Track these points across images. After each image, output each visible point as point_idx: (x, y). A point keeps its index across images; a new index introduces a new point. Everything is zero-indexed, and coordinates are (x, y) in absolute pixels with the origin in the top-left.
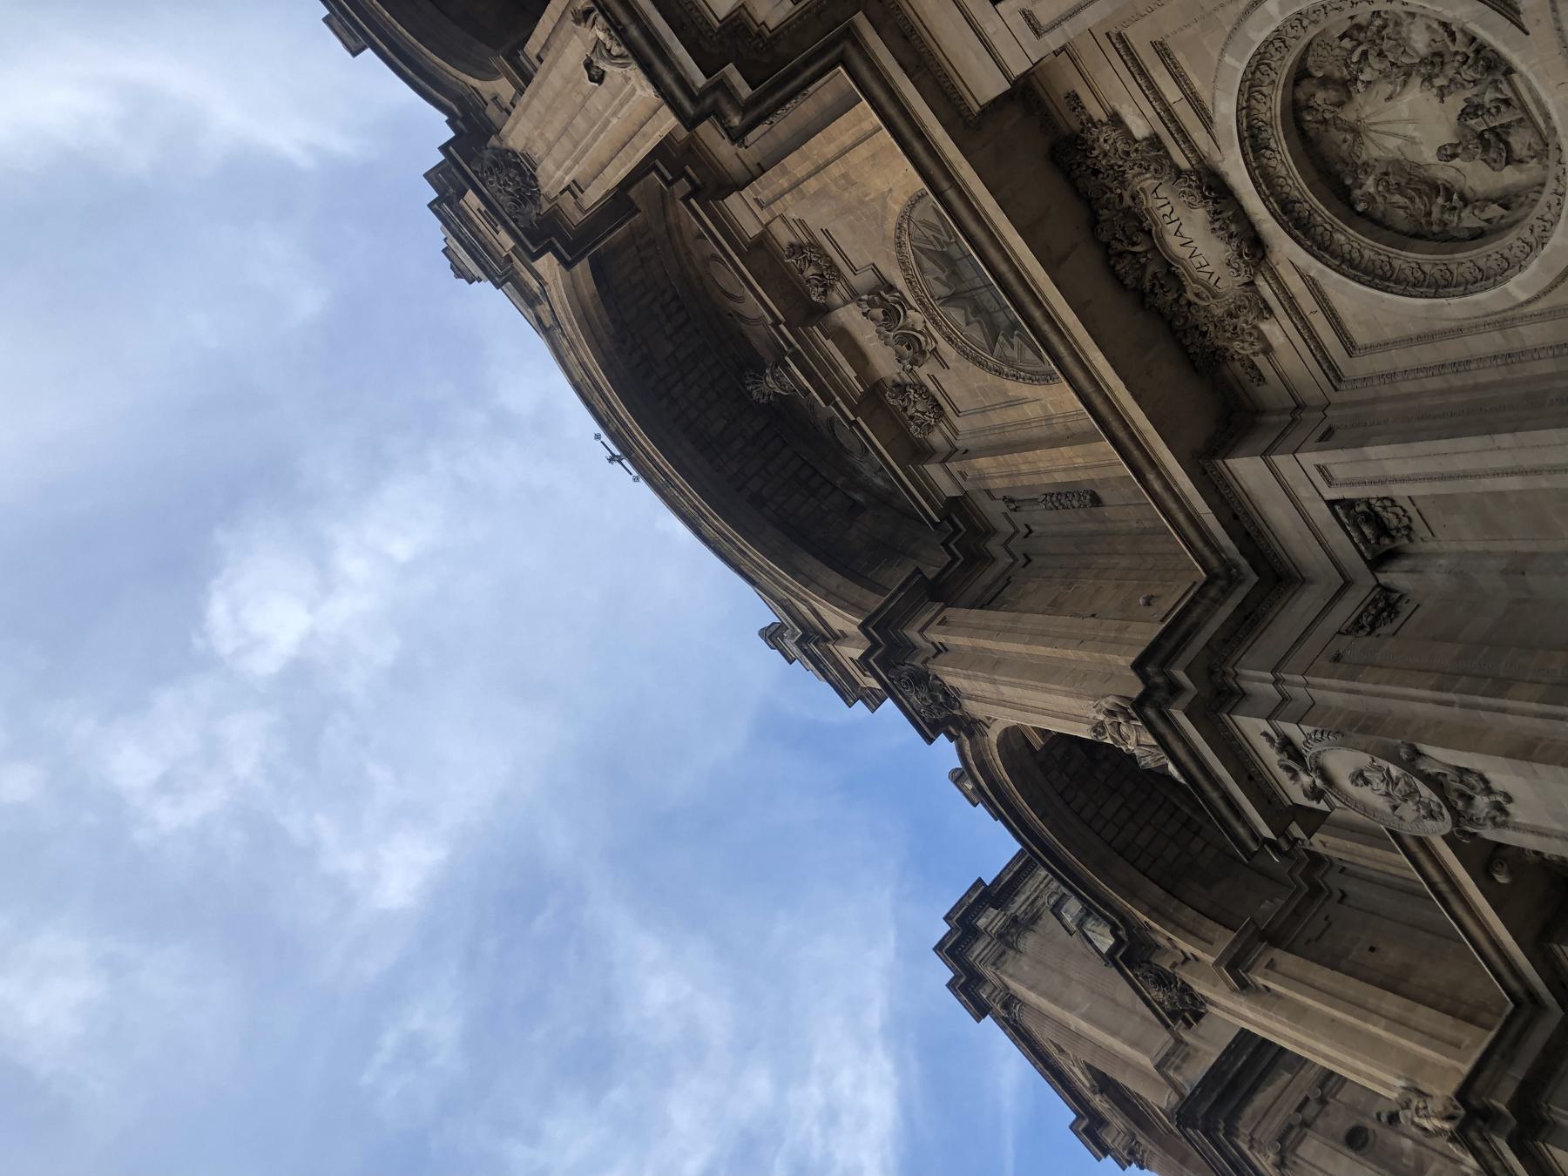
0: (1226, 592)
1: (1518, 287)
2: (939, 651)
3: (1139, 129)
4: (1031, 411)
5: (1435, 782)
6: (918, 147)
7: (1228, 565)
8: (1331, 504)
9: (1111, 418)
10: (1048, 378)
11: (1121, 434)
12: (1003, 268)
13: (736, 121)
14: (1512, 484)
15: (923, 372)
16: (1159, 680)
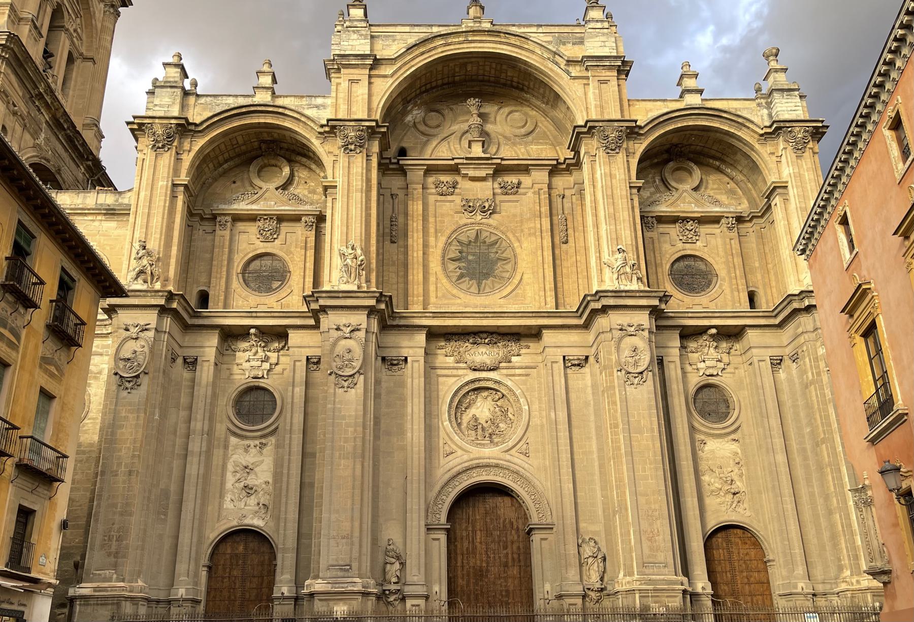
0: (389, 315)
1: (447, 423)
2: (367, 156)
3: (514, 359)
4: (432, 240)
5: (352, 376)
6: (546, 315)
7: (394, 318)
8: (406, 359)
9: (453, 315)
10: (443, 257)
11: (447, 315)
12: (506, 315)
13: (589, 298)
14: (409, 410)
15: (457, 199)
16: (383, 299)
